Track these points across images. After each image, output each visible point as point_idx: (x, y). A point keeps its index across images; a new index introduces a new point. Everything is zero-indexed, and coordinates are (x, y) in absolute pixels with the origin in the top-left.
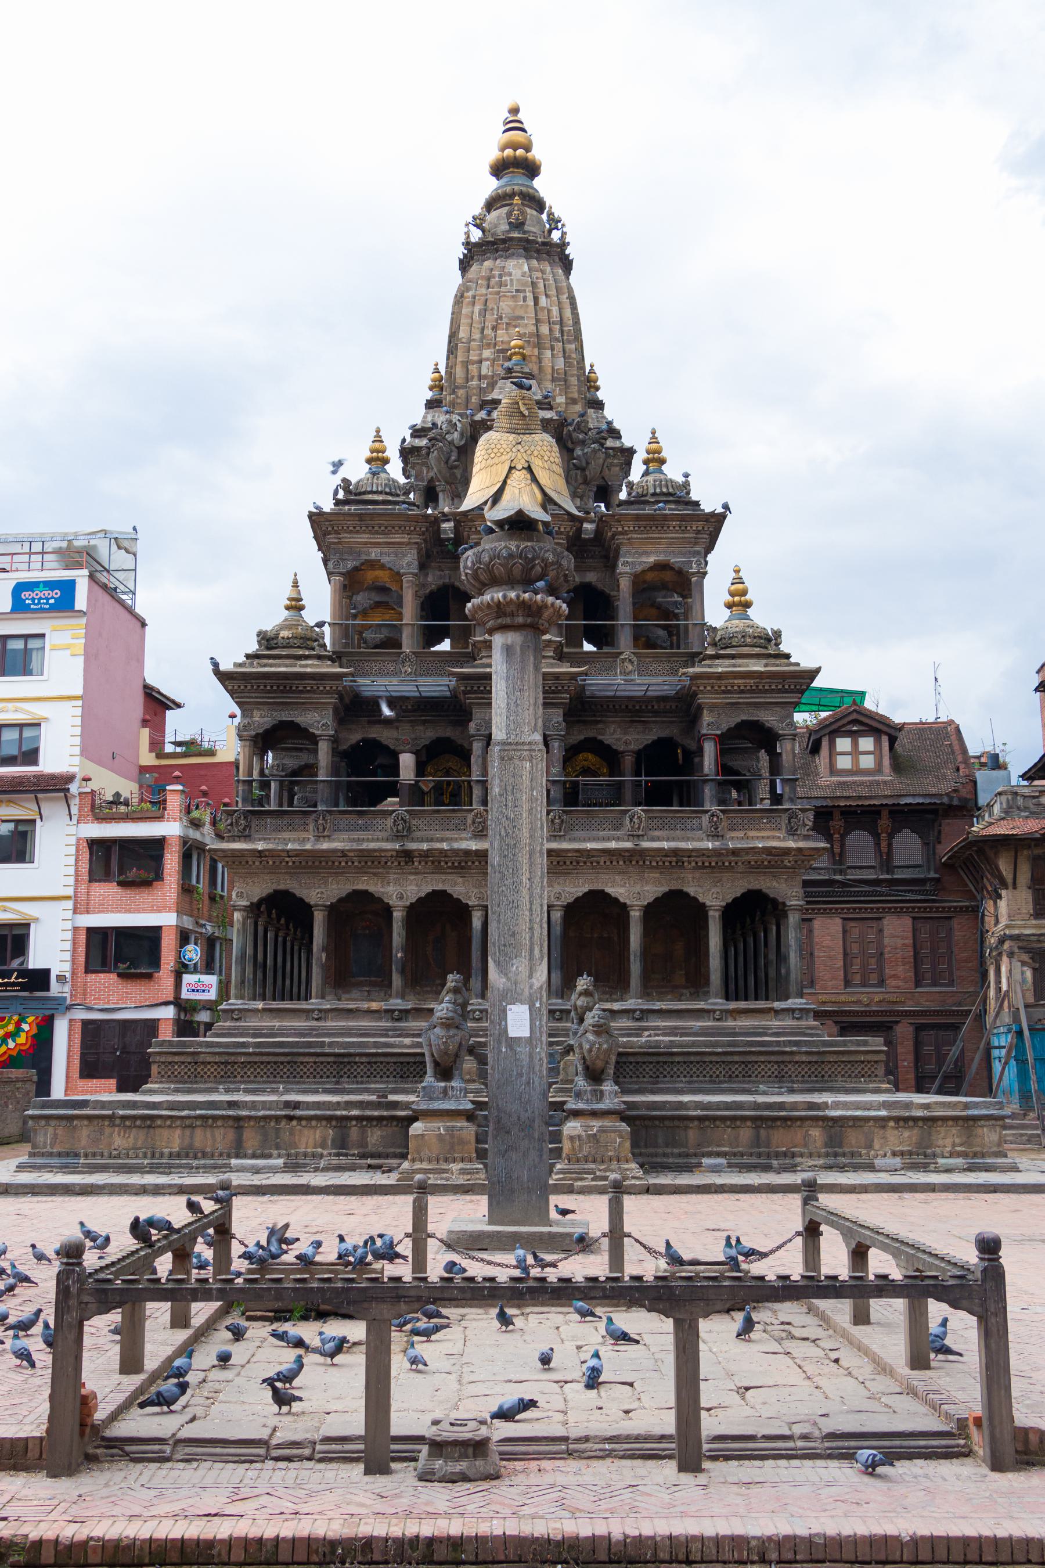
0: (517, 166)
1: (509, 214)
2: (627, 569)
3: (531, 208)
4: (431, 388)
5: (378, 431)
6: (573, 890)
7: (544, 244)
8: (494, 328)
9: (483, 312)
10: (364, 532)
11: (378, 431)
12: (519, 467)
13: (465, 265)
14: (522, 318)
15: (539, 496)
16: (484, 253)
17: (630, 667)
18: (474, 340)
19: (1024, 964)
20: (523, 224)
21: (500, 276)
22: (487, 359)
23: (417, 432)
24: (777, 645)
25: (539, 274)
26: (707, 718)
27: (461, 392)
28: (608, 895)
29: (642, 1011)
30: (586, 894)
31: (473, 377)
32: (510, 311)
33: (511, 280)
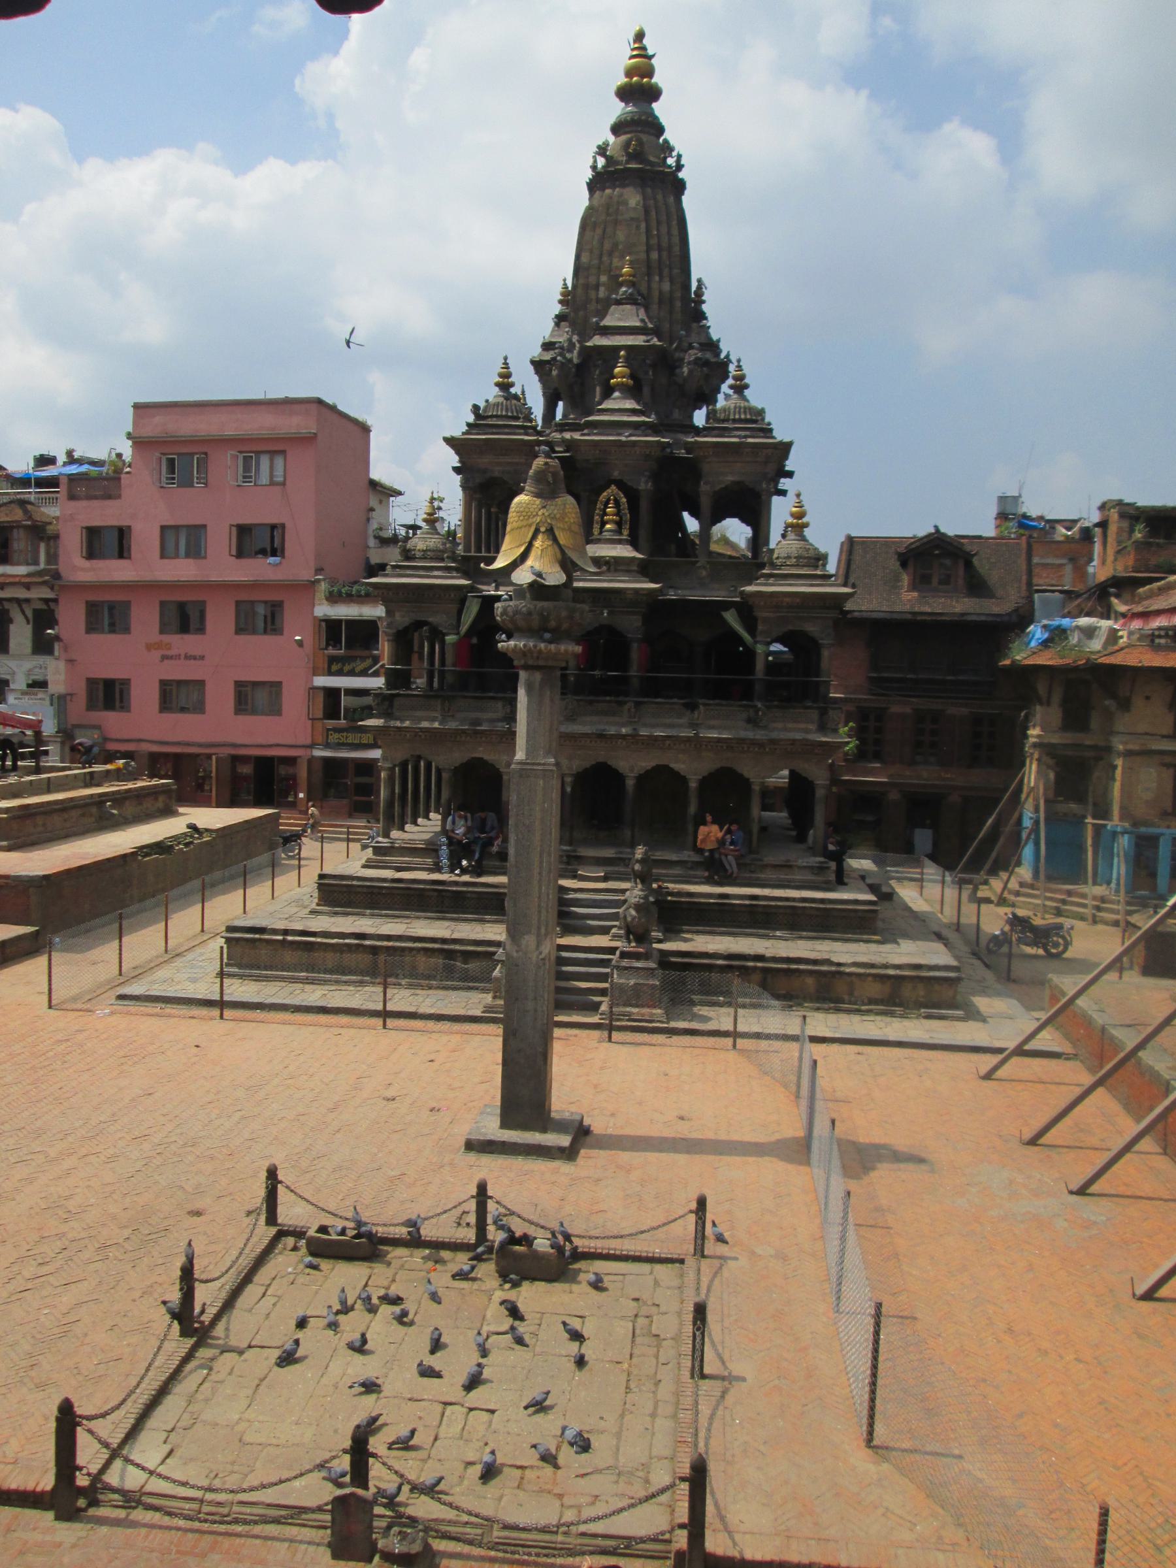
0: (640, 90)
3: (648, 133)
4: (560, 302)
5: (506, 358)
6: (644, 764)
11: (506, 358)
12: (543, 529)
13: (593, 186)
15: (559, 555)
17: (704, 573)
19: (1049, 767)
23: (547, 346)
24: (824, 565)
26: (760, 627)
27: (581, 313)
28: (672, 769)
29: (693, 862)
30: (653, 768)
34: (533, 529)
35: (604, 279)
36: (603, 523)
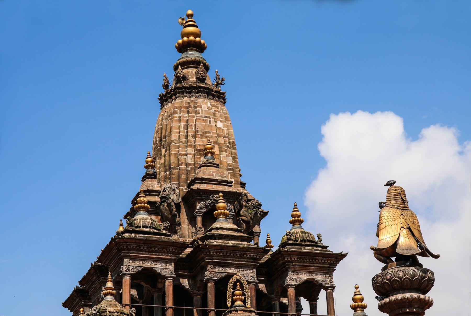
1: (197, 73)
2: (293, 283)
7: (216, 92)
8: (195, 137)
9: (187, 127)
10: (145, 251)
14: (210, 133)
16: (183, 93)
18: (181, 142)
20: (205, 79)
21: (195, 107)
22: (190, 154)
25: (216, 109)
31: (182, 163)
32: (202, 128)
33: (202, 110)
34: (399, 227)
35: (190, 150)
36: (233, 302)
